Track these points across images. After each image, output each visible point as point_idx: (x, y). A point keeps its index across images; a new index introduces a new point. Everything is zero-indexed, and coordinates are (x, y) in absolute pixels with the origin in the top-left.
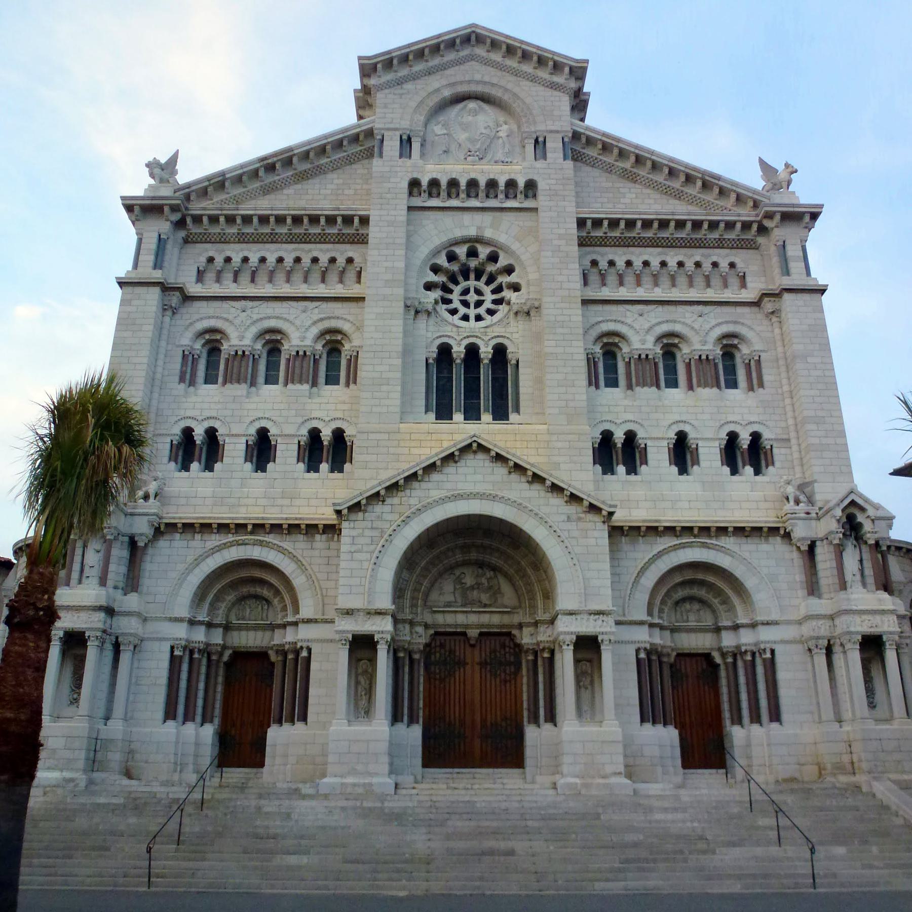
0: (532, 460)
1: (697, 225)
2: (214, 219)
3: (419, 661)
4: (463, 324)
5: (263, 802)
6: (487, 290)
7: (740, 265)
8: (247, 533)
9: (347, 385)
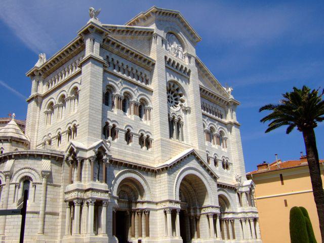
2: (113, 44)
6: (174, 98)
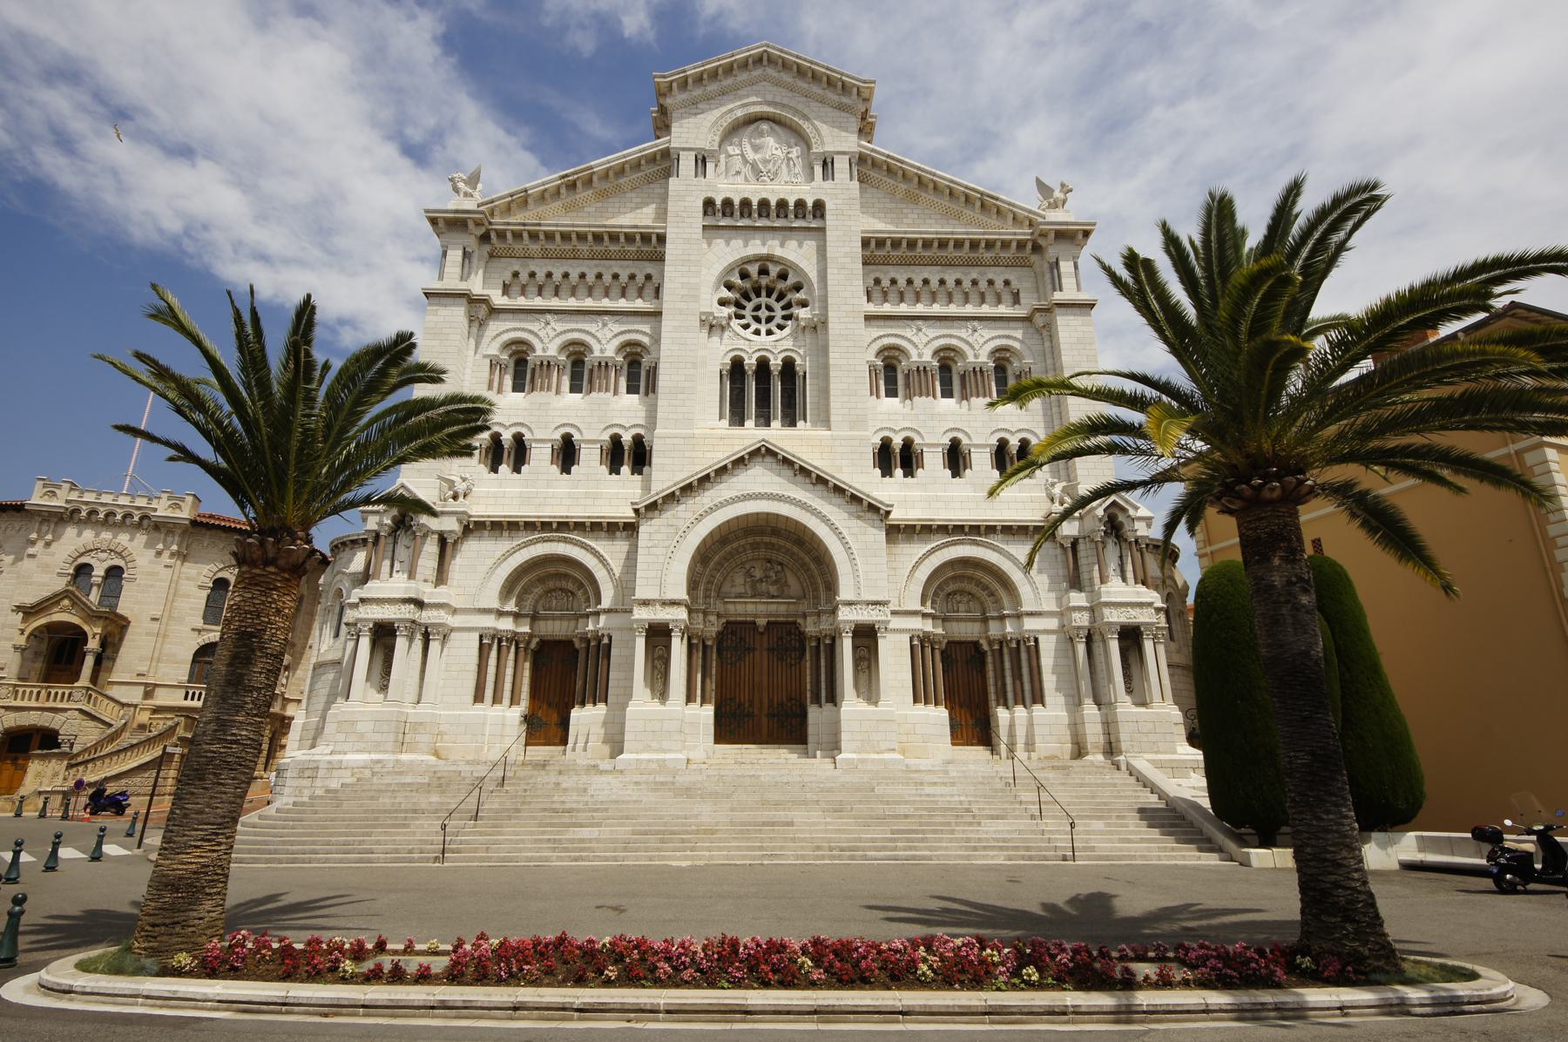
0: (815, 463)
1: (974, 245)
2: (518, 236)
3: (712, 647)
4: (755, 337)
5: (561, 778)
6: (777, 306)
7: (1015, 284)
8: (552, 531)
9: (647, 394)
